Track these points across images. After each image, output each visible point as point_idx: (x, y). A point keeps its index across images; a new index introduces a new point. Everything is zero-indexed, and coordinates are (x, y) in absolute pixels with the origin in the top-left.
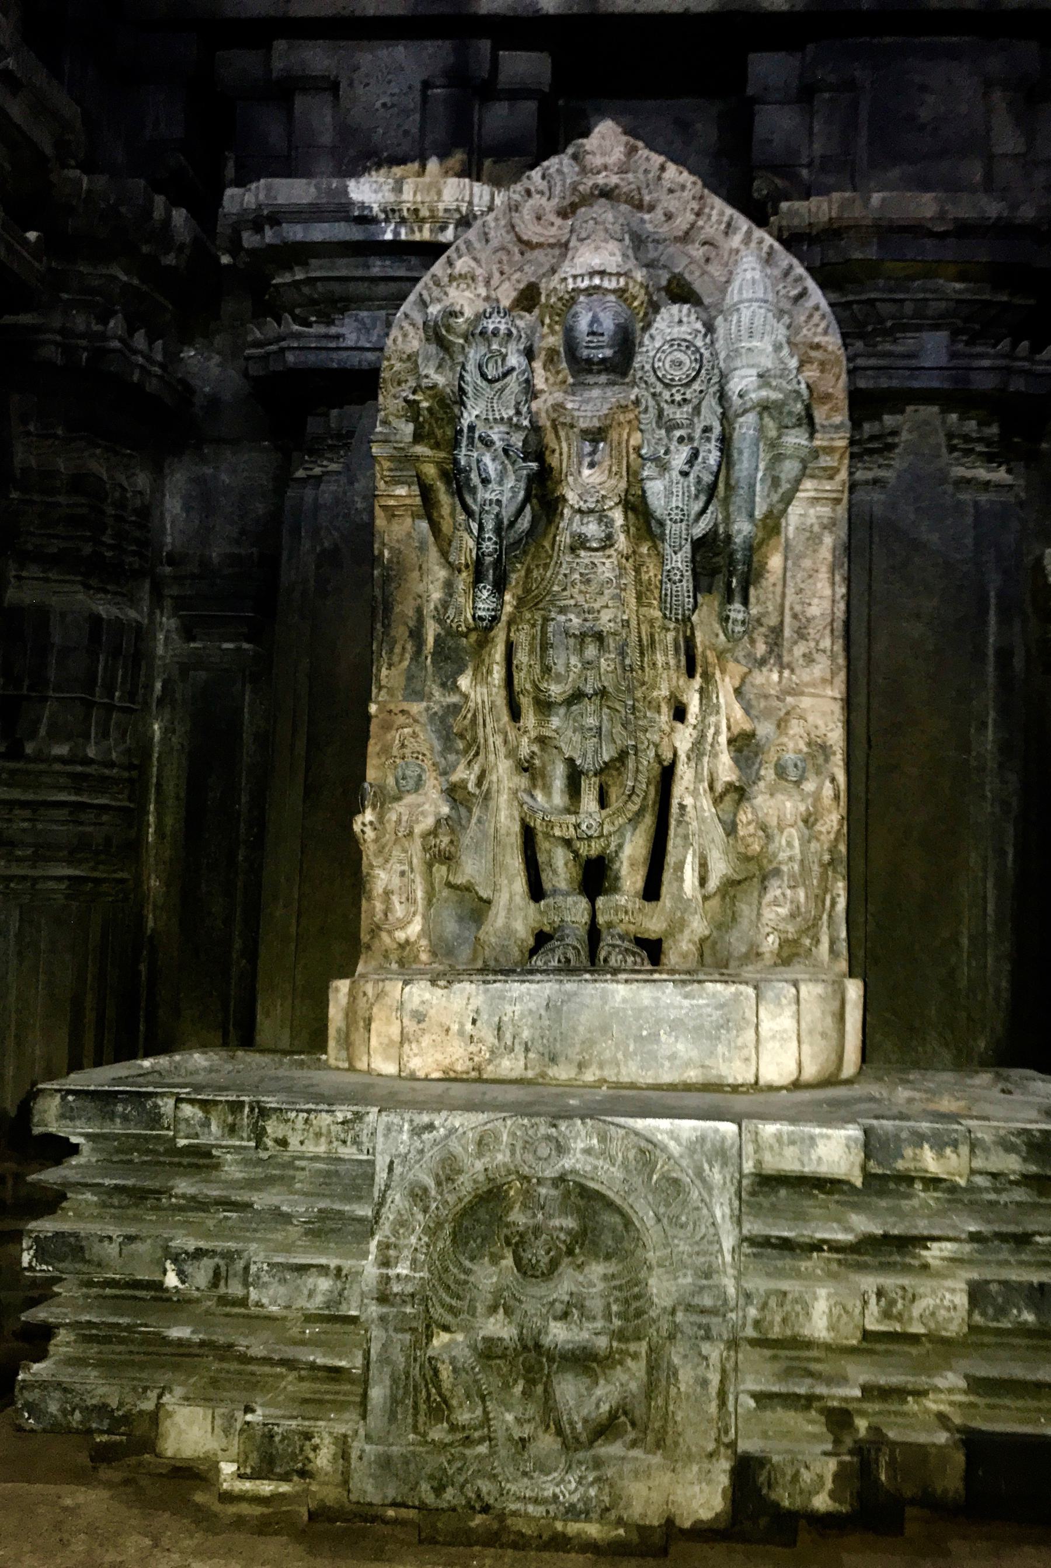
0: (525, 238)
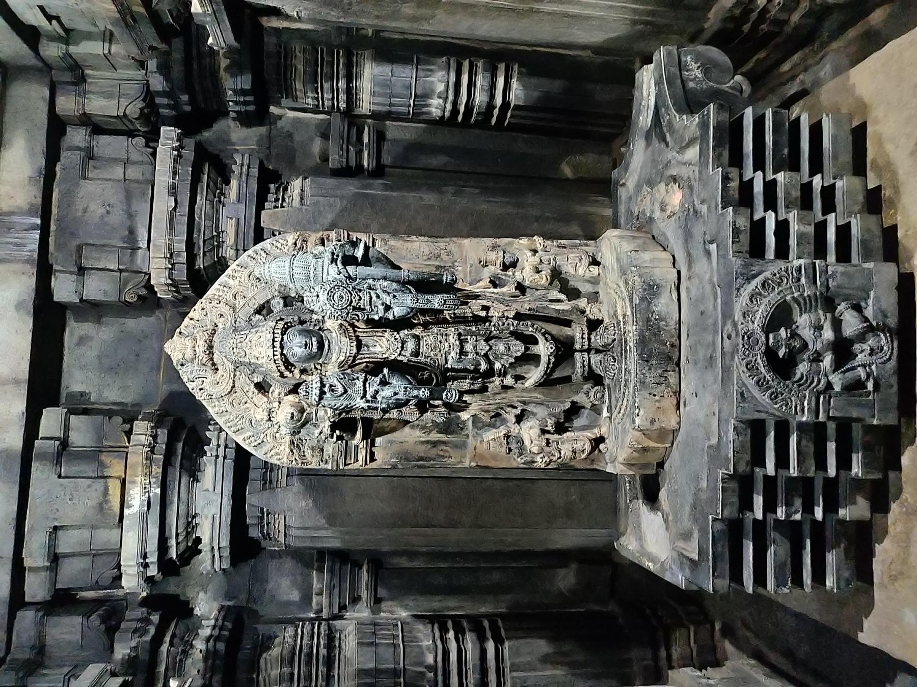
0: (229, 390)
